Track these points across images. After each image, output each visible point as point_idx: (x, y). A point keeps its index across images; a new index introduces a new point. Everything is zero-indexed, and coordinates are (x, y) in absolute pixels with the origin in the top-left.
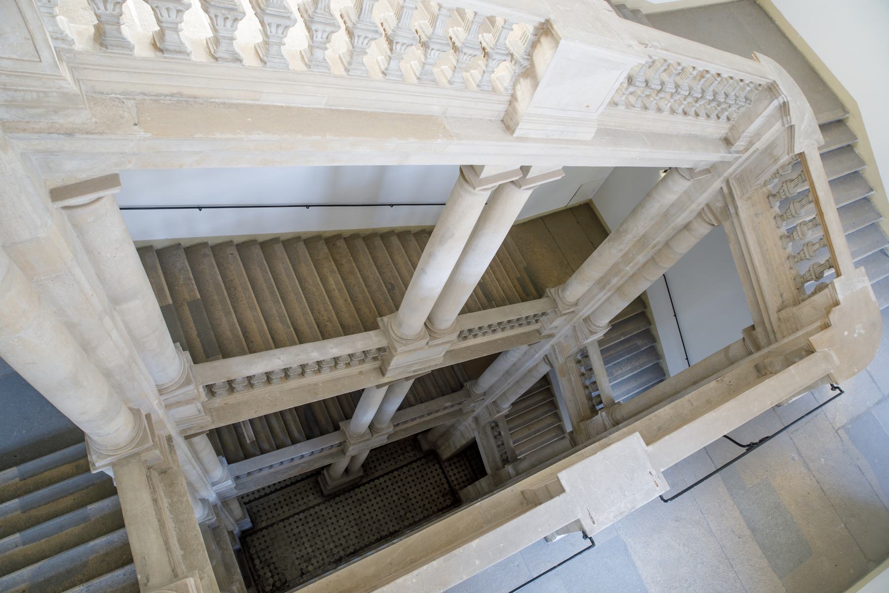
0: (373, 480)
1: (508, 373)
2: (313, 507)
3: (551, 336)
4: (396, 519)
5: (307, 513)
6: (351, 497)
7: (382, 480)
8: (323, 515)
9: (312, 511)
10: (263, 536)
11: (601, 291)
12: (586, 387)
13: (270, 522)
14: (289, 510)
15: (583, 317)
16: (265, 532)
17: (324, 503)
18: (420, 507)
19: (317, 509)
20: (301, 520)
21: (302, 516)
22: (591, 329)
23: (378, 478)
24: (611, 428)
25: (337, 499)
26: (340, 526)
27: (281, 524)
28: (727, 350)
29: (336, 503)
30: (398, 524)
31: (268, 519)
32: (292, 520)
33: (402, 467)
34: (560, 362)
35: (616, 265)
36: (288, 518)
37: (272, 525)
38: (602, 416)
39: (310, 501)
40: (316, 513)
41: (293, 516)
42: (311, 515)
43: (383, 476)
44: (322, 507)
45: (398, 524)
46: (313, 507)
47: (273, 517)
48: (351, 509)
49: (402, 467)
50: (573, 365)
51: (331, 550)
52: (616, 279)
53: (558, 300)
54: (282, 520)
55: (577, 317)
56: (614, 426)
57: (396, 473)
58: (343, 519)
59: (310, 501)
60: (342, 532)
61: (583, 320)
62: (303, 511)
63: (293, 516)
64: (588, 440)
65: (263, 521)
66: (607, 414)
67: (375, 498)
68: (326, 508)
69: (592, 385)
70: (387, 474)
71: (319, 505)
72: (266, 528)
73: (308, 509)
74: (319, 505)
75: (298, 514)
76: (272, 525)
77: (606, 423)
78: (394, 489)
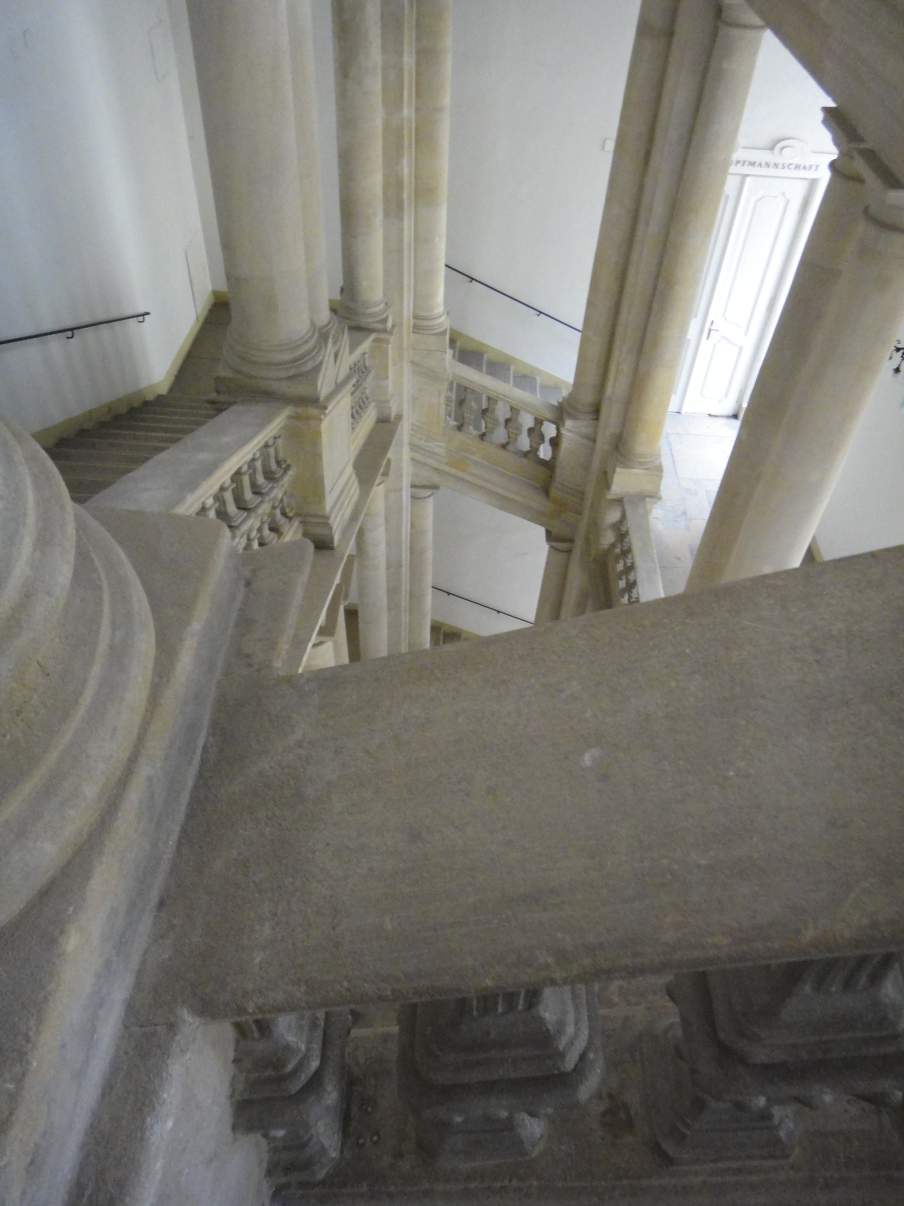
1: (393, 591)
3: (399, 417)
11: (402, 220)
12: (504, 446)
15: (411, 330)
22: (435, 332)
24: (596, 427)
28: (644, 29)
34: (442, 451)
35: (387, 126)
38: (570, 431)
50: (460, 436)
52: (405, 161)
53: (364, 322)
55: (405, 327)
56: (597, 419)
61: (413, 332)
64: (582, 499)
66: (573, 417)
69: (510, 424)
77: (583, 430)
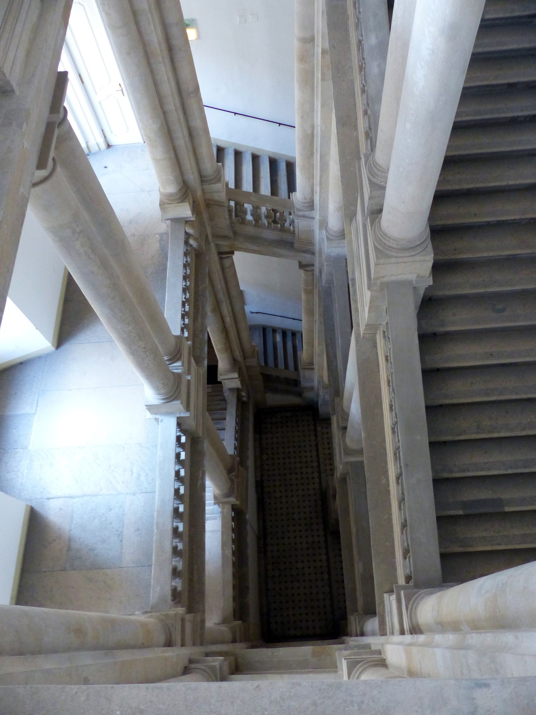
0: (327, 547)
2: (320, 477)
4: (278, 557)
6: (317, 518)
7: (324, 557)
9: (316, 475)
10: (309, 425)
14: (325, 454)
18: (280, 589)
19: (317, 480)
20: (312, 462)
21: (315, 464)
23: (327, 554)
26: (292, 496)
30: (273, 557)
32: (314, 454)
33: (330, 586)
36: (317, 450)
37: (316, 436)
40: (313, 478)
41: (318, 456)
42: (313, 473)
43: (328, 560)
45: (273, 557)
46: (320, 477)
47: (323, 438)
48: (305, 513)
49: (330, 586)
54: (317, 445)
57: (326, 576)
62: (319, 466)
63: (318, 456)
65: (322, 428)
67: (307, 543)
68: (314, 489)
70: (328, 567)
71: (320, 483)
72: (315, 430)
73: (319, 472)
74: (320, 483)
75: (318, 462)
76: (316, 436)
78: (309, 568)
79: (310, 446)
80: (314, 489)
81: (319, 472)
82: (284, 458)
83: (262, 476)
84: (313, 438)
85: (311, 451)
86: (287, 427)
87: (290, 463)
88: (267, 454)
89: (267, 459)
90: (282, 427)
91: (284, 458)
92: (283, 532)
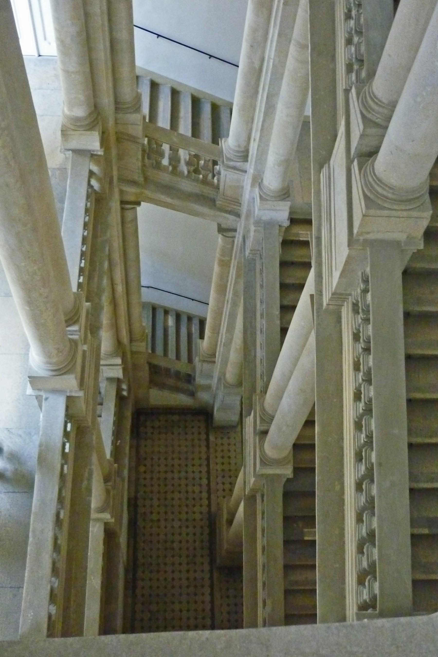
2: (209, 499)
5: (205, 488)
6: (202, 548)
8: (194, 506)
9: (205, 495)
10: (199, 433)
13: (212, 445)
16: (203, 436)
17: (209, 512)
19: (205, 502)
21: (204, 481)
25: (207, 531)
26: (173, 520)
27: (204, 456)
29: (202, 527)
31: (216, 445)
36: (208, 465)
37: (208, 446)
39: (218, 497)
41: (208, 472)
44: (204, 509)
46: (209, 499)
51: (152, 499)
54: (208, 459)
58: (180, 527)
59: (218, 497)
60: (166, 520)
62: (209, 485)
63: (208, 472)
68: (201, 513)
71: (209, 505)
72: (207, 440)
73: (209, 492)
74: (209, 505)
75: (208, 479)
76: (208, 446)
79: (200, 458)
80: (201, 513)
81: (209, 492)
82: (166, 472)
83: (137, 491)
84: (204, 449)
85: (200, 465)
86: (173, 433)
87: (173, 478)
88: (145, 466)
89: (145, 472)
90: (166, 434)
91: (166, 472)
92: (158, 564)
